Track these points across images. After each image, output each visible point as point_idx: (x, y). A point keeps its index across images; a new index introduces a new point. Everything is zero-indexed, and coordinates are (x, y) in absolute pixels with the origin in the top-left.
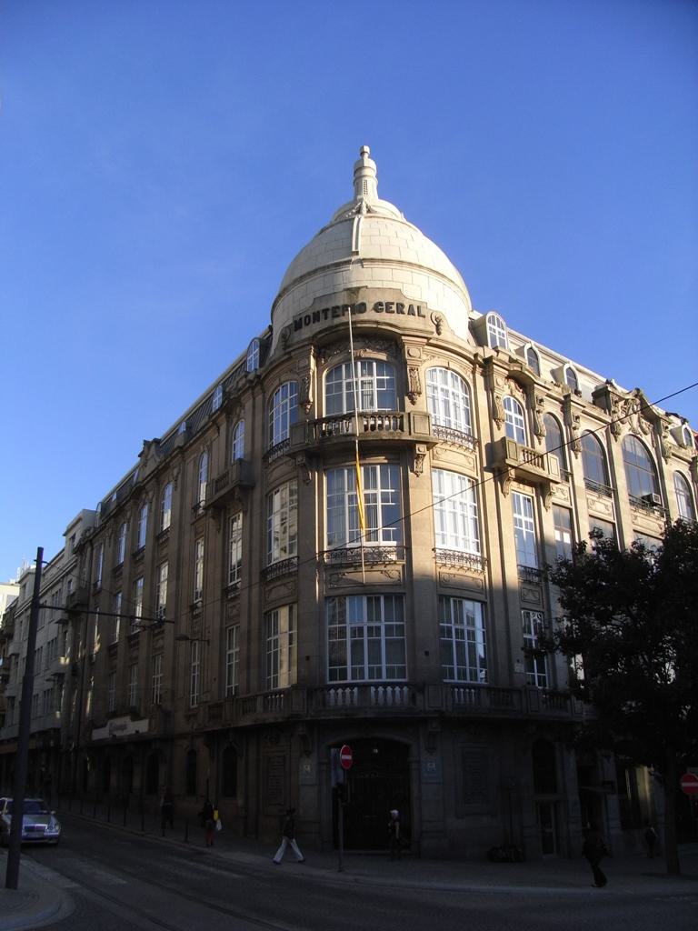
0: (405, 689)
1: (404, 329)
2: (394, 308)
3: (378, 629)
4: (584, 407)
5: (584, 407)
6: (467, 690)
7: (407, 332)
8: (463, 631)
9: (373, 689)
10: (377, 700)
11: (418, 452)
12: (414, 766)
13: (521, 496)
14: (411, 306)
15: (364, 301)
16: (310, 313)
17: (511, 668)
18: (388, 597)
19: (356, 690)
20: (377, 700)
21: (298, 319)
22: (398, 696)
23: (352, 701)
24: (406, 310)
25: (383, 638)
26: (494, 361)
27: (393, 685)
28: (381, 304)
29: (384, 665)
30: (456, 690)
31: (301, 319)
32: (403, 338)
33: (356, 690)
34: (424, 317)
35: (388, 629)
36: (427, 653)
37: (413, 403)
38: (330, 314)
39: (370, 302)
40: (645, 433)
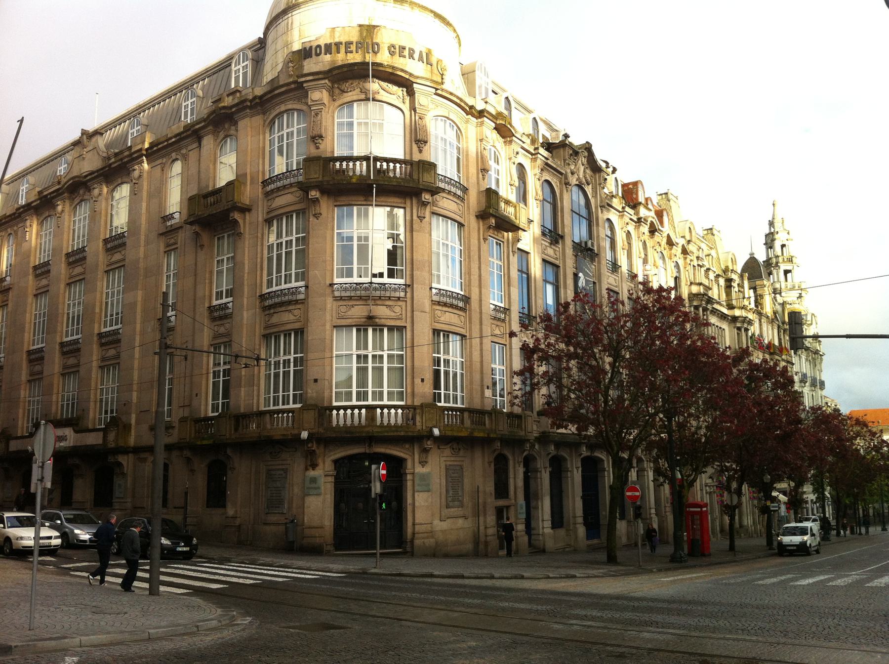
0: (400, 411)
2: (406, 53)
3: (381, 357)
4: (524, 142)
5: (524, 142)
6: (450, 413)
8: (448, 361)
9: (379, 411)
10: (382, 421)
11: (423, 200)
12: (409, 477)
13: (495, 240)
16: (322, 43)
17: (483, 393)
18: (391, 329)
19: (364, 411)
20: (382, 421)
21: (308, 46)
22: (395, 417)
23: (360, 421)
24: (416, 56)
25: (385, 365)
26: (486, 114)
27: (389, 407)
29: (385, 390)
30: (446, 412)
31: (311, 47)
35: (389, 356)
36: (423, 380)
37: (420, 151)
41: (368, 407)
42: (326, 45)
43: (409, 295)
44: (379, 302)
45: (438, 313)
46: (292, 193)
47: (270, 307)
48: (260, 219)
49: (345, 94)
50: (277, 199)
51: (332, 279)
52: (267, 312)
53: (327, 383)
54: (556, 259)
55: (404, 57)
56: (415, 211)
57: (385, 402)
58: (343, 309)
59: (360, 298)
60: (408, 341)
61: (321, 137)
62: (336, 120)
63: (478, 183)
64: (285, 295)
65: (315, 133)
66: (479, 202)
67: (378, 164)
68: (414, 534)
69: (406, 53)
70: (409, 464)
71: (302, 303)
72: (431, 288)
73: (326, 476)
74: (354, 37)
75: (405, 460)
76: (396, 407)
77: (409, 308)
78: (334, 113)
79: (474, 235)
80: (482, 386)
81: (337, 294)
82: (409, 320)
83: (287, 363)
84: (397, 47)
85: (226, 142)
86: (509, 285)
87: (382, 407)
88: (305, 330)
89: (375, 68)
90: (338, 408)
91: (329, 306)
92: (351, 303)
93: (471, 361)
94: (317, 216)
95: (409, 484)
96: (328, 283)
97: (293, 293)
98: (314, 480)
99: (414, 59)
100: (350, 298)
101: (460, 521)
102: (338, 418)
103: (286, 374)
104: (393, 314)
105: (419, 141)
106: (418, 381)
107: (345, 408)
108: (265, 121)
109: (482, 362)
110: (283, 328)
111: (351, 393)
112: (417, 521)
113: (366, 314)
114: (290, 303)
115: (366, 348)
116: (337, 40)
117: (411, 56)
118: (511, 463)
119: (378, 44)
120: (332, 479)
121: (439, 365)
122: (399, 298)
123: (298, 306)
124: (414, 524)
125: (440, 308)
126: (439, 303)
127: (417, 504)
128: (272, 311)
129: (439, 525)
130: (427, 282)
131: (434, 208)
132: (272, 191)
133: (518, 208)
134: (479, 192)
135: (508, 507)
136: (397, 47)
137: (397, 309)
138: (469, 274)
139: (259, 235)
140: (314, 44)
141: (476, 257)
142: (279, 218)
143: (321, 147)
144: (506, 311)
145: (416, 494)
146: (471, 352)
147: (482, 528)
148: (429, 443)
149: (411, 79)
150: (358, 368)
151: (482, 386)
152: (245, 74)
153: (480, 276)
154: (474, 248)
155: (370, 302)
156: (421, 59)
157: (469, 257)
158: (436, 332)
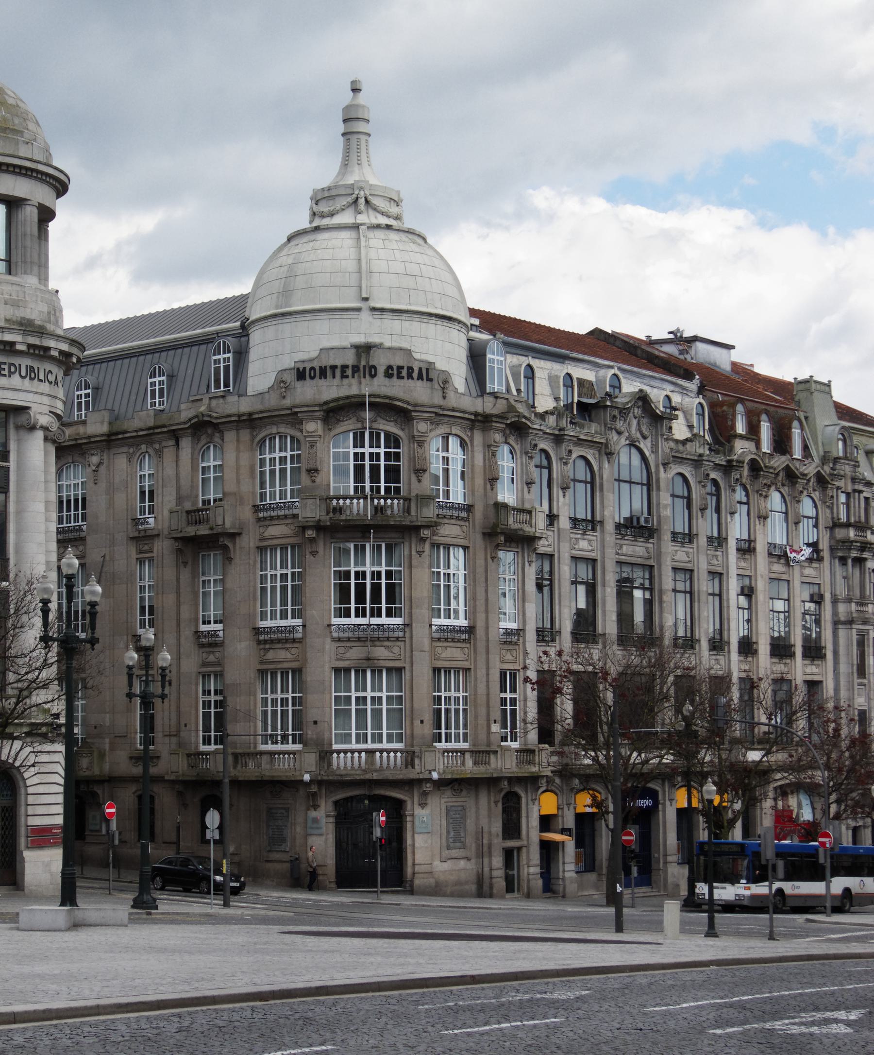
0: (399, 754)
1: (416, 405)
2: (404, 373)
3: (380, 698)
7: (417, 409)
9: (378, 754)
12: (409, 819)
14: (420, 369)
15: (374, 364)
16: (316, 364)
17: (489, 727)
18: (389, 670)
24: (415, 375)
25: (384, 707)
28: (390, 367)
29: (385, 732)
31: (304, 369)
32: (413, 414)
33: (363, 754)
34: (431, 380)
35: (388, 697)
36: (422, 722)
37: (419, 481)
38: (338, 373)
39: (381, 361)
40: (645, 438)
41: (368, 751)
42: (321, 367)
43: (407, 635)
44: (377, 643)
45: (439, 650)
46: (287, 525)
47: (265, 642)
48: (252, 545)
49: (342, 424)
50: (270, 528)
51: (330, 619)
52: (262, 647)
53: (326, 724)
54: (592, 551)
55: (403, 378)
56: (413, 546)
57: (385, 745)
58: (341, 650)
59: (359, 639)
60: (407, 682)
61: (316, 470)
62: (332, 450)
63: (485, 495)
64: (282, 632)
65: (312, 466)
66: (486, 517)
67: (376, 501)
68: (414, 874)
69: (404, 373)
70: (409, 806)
71: (300, 642)
72: (431, 625)
73: (327, 816)
74: (349, 359)
75: (405, 801)
76: (395, 751)
77: (408, 648)
78: (329, 443)
79: (481, 555)
80: (488, 720)
81: (335, 635)
82: (408, 660)
83: (284, 701)
84: (395, 368)
85: (209, 448)
86: (524, 601)
87: (381, 751)
88: (304, 670)
89: (373, 399)
90: (338, 752)
91: (327, 647)
92: (349, 644)
93: (476, 694)
94: (314, 553)
95: (409, 825)
96: (327, 623)
97: (290, 632)
98: (316, 820)
99: (413, 379)
100: (349, 639)
101: (462, 863)
102: (339, 762)
103: (284, 713)
104: (392, 655)
105: (418, 470)
106: (417, 723)
107: (345, 752)
108: (252, 440)
109: (488, 695)
110: (279, 666)
111: (350, 735)
112: (417, 862)
113: (364, 655)
114: (287, 640)
115: (365, 690)
116: (332, 362)
117: (410, 376)
118: (524, 801)
119: (374, 367)
120: (332, 820)
121: (440, 704)
122: (397, 639)
123: (296, 645)
124: (414, 865)
125: (441, 644)
126: (439, 639)
127: (417, 845)
128: (267, 646)
129: (440, 867)
130: (427, 620)
131: (435, 538)
132: (265, 518)
133: (533, 514)
134: (486, 506)
135: (519, 849)
136: (395, 368)
137: (396, 650)
138: (474, 599)
139: (251, 562)
140: (308, 366)
141: (483, 579)
142: (273, 548)
143: (318, 480)
144: (520, 632)
145: (416, 835)
146: (476, 686)
147: (486, 869)
148: (428, 785)
149: (410, 407)
150: (357, 710)
151: (488, 720)
152: (227, 368)
153: (487, 600)
154: (480, 570)
155: (368, 643)
156: (420, 377)
157: (474, 581)
158: (436, 671)
